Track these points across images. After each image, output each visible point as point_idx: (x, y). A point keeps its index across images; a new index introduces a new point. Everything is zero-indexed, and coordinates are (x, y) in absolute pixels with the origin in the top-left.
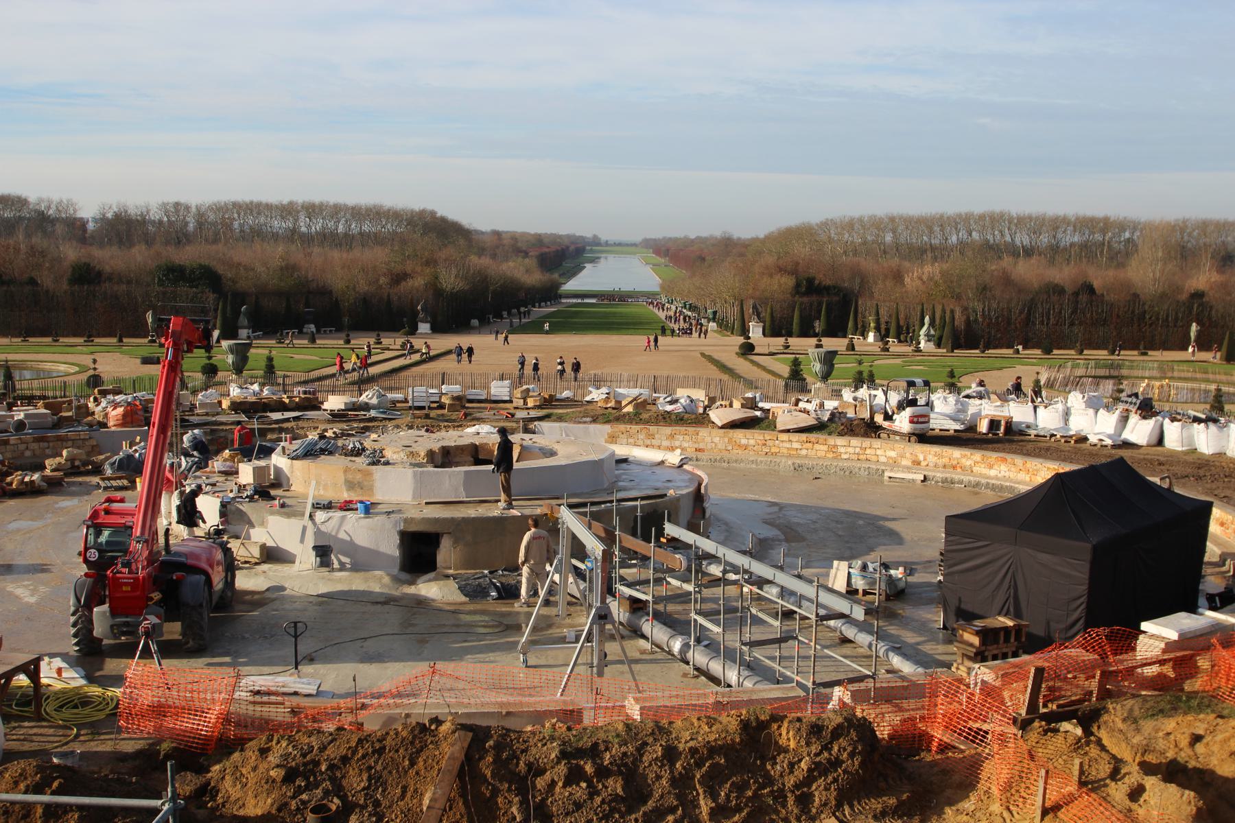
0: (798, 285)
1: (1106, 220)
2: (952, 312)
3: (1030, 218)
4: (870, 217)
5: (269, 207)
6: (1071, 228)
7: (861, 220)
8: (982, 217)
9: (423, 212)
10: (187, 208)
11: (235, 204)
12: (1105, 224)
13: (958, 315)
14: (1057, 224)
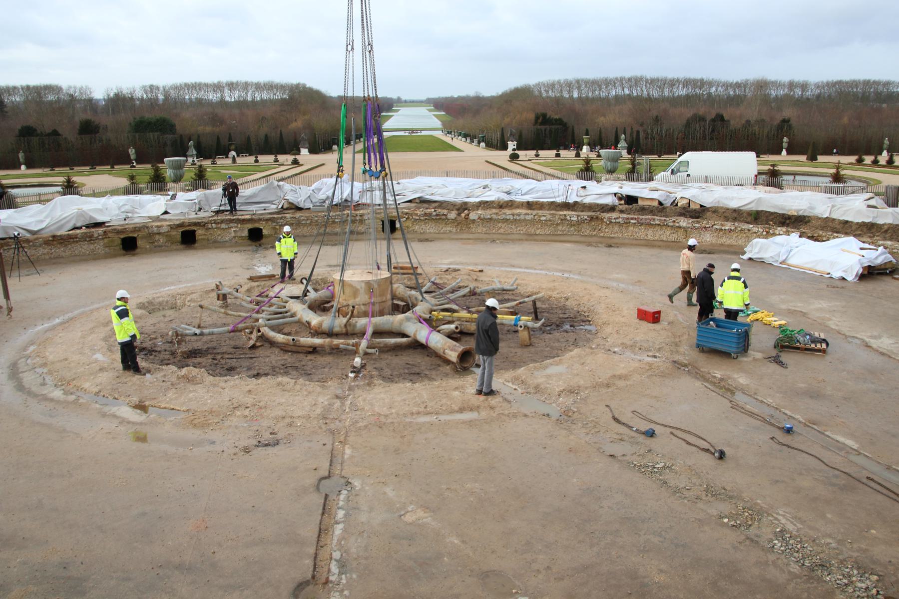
0: (537, 118)
1: (702, 81)
2: (638, 132)
3: (658, 80)
4: (565, 81)
5: (206, 85)
6: (681, 85)
7: (559, 82)
8: (630, 79)
9: (298, 85)
10: (158, 88)
11: (186, 85)
12: (701, 83)
13: (641, 134)
14: (673, 83)
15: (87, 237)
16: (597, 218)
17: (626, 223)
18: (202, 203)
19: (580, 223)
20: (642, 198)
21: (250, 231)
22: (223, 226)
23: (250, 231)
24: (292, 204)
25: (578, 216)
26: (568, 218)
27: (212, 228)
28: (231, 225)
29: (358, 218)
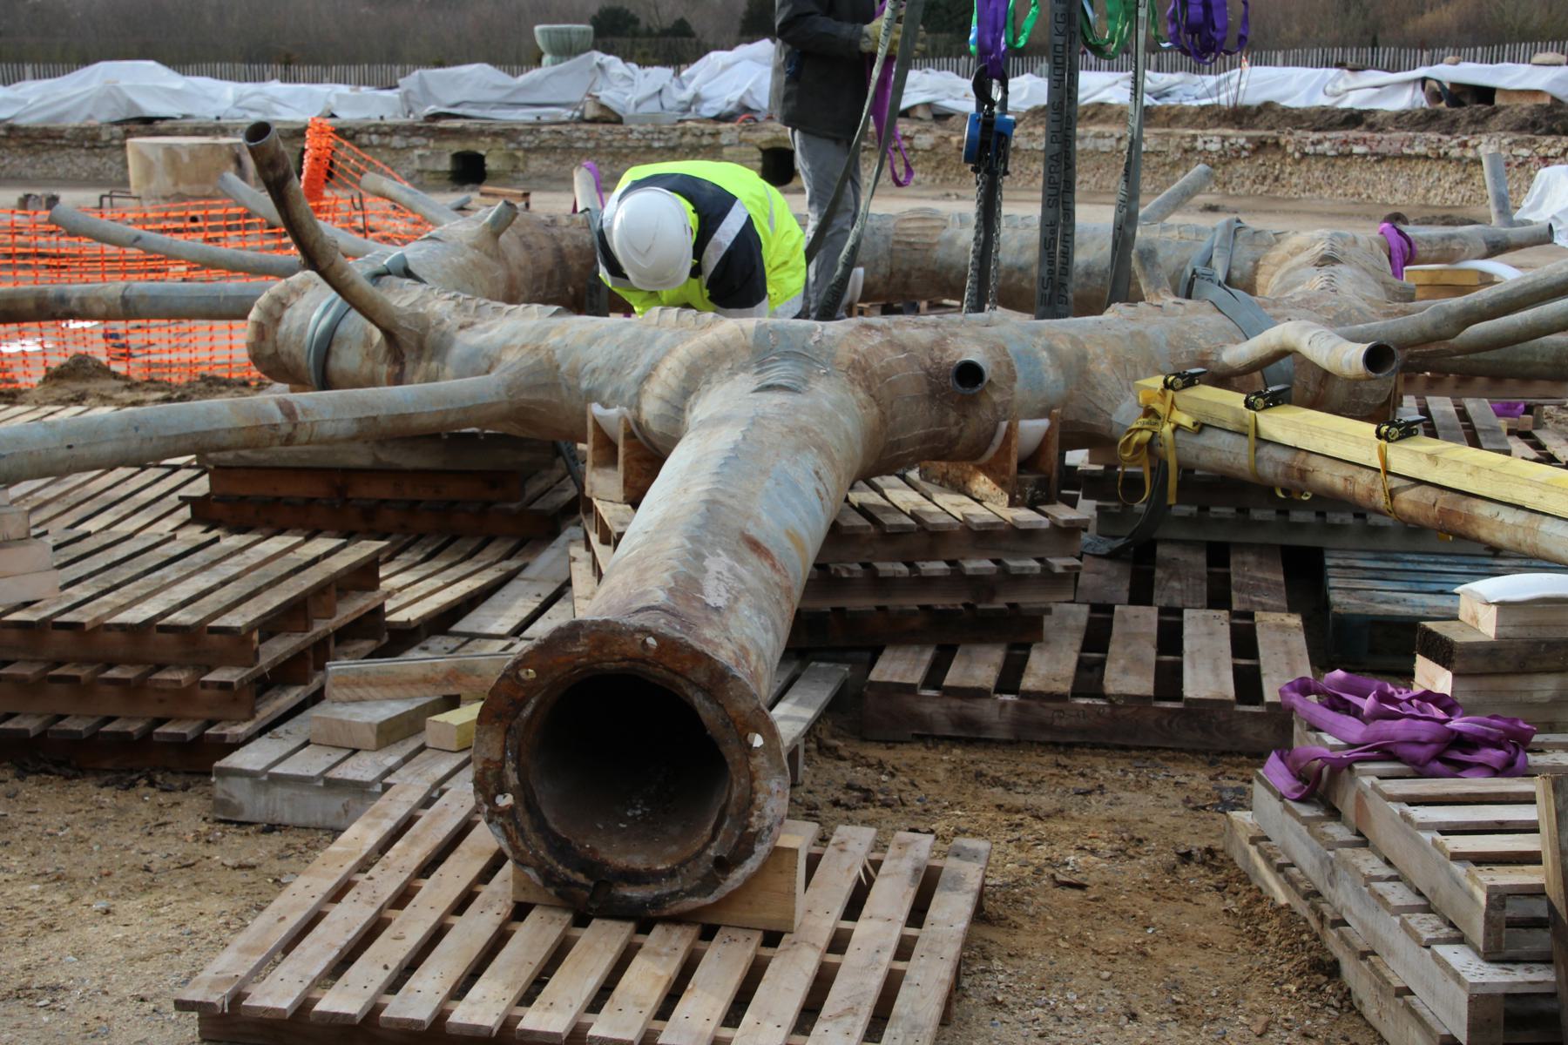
15: (86, 138)
16: (1277, 144)
17: (1341, 156)
18: (411, 97)
19: (1228, 157)
20: (1507, 93)
21: (458, 157)
22: (397, 141)
23: (458, 157)
24: (603, 107)
25: (1224, 138)
26: (1199, 144)
27: (370, 145)
28: (414, 140)
29: (706, 141)
